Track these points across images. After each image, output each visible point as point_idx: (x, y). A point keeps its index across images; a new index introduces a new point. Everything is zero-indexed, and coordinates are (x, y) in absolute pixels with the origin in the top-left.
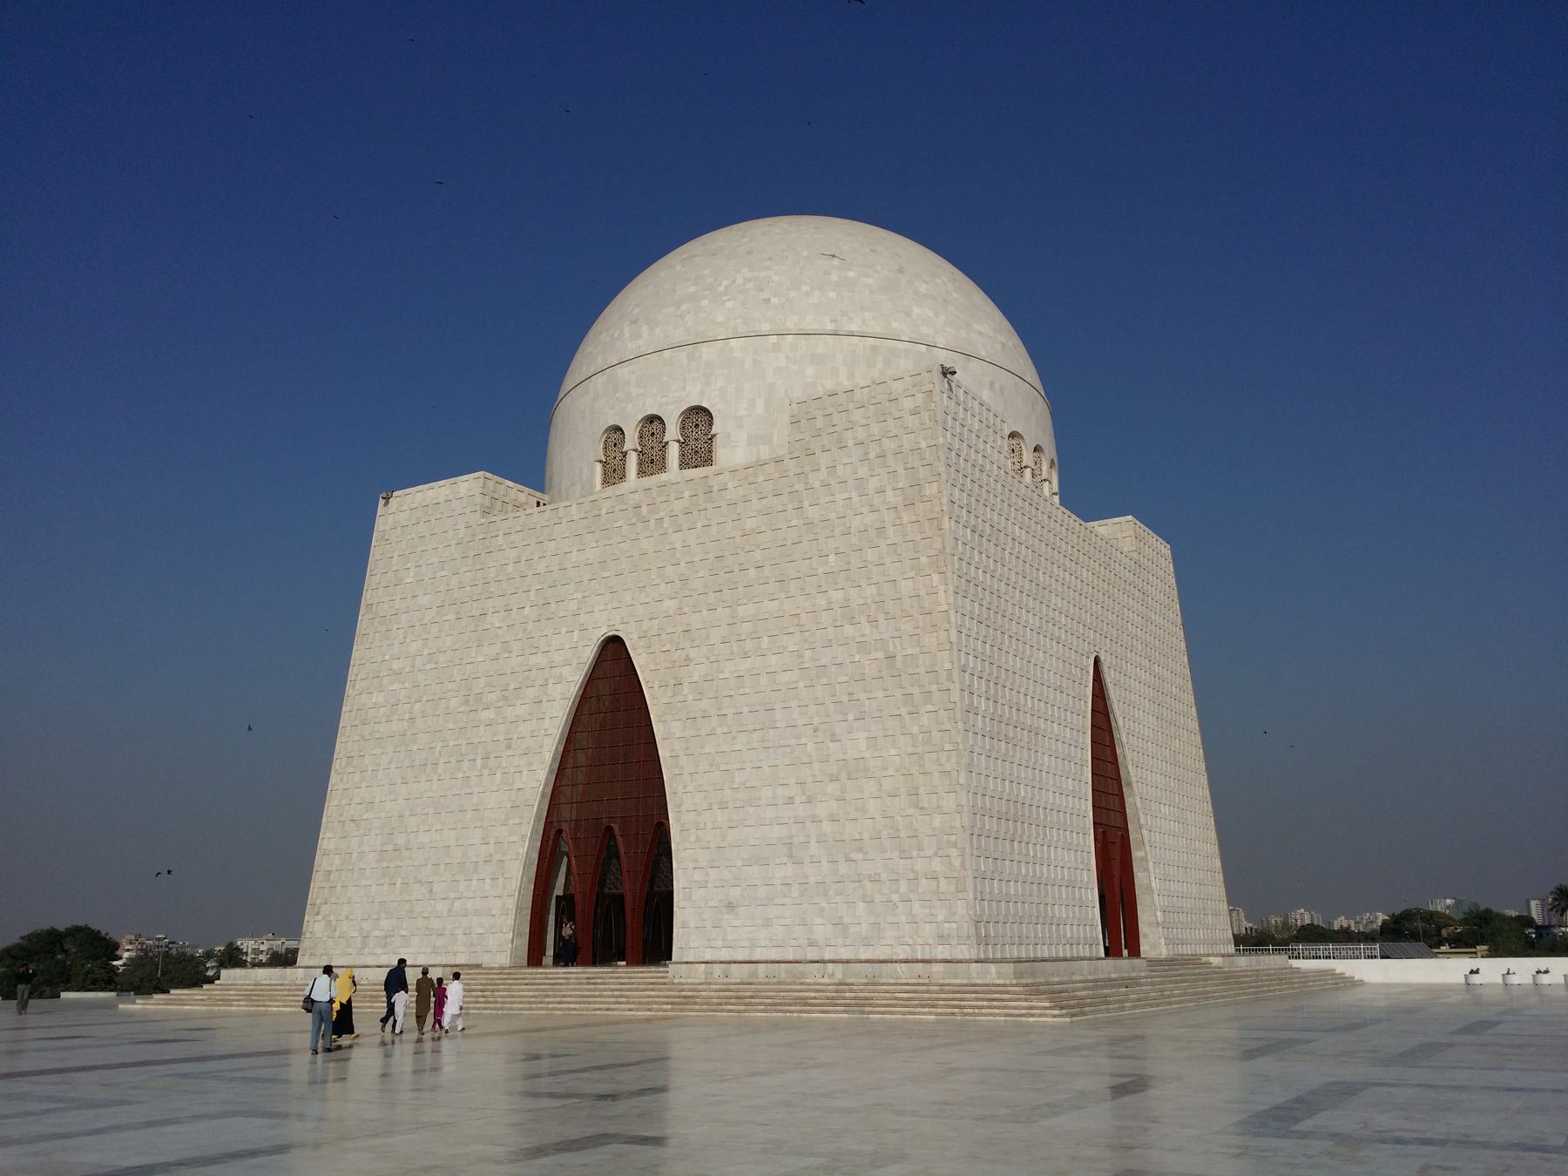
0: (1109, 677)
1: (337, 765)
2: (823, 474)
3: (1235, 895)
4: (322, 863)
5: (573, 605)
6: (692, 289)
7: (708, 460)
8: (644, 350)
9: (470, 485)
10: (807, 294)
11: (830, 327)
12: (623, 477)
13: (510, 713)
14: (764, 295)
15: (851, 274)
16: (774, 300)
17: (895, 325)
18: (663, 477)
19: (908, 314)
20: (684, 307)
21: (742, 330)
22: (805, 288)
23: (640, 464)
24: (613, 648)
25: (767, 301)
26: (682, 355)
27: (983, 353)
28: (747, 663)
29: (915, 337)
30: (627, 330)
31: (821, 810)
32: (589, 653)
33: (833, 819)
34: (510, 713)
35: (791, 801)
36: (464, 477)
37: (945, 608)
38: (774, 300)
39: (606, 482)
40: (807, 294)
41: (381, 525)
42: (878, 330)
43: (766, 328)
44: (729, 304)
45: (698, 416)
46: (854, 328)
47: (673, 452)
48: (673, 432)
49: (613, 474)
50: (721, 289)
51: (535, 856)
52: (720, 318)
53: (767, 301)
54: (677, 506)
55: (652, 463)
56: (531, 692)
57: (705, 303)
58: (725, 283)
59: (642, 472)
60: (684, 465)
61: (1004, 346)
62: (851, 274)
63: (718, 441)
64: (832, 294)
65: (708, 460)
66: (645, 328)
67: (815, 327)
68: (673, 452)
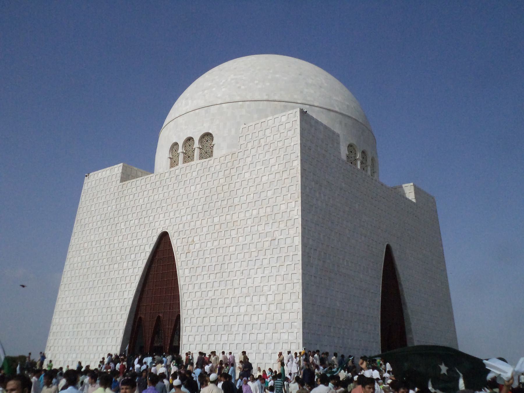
0: (396, 254)
1: (62, 287)
2: (250, 159)
3: (304, 344)
4: (54, 328)
6: (210, 84)
7: (211, 155)
9: (117, 169)
10: (257, 84)
11: (265, 98)
14: (238, 85)
15: (277, 76)
16: (243, 87)
17: (295, 96)
18: (192, 163)
19: (302, 92)
20: (206, 92)
22: (256, 82)
23: (184, 158)
24: (164, 237)
25: (239, 87)
26: (203, 111)
27: (337, 109)
28: (216, 243)
29: (304, 102)
30: (184, 102)
31: (243, 309)
32: (155, 239)
36: (116, 166)
37: (297, 217)
38: (243, 87)
39: (172, 166)
40: (257, 84)
41: (85, 187)
42: (287, 100)
43: (238, 98)
44: (223, 90)
45: (207, 136)
46: (276, 98)
47: (197, 153)
48: (196, 144)
49: (173, 163)
50: (221, 83)
51: (131, 328)
52: (219, 95)
53: (239, 87)
54: (195, 174)
55: (188, 157)
57: (214, 89)
58: (224, 81)
59: (185, 161)
60: (201, 157)
61: (348, 106)
62: (277, 76)
64: (268, 84)
66: (190, 102)
67: (259, 98)
68: (197, 153)
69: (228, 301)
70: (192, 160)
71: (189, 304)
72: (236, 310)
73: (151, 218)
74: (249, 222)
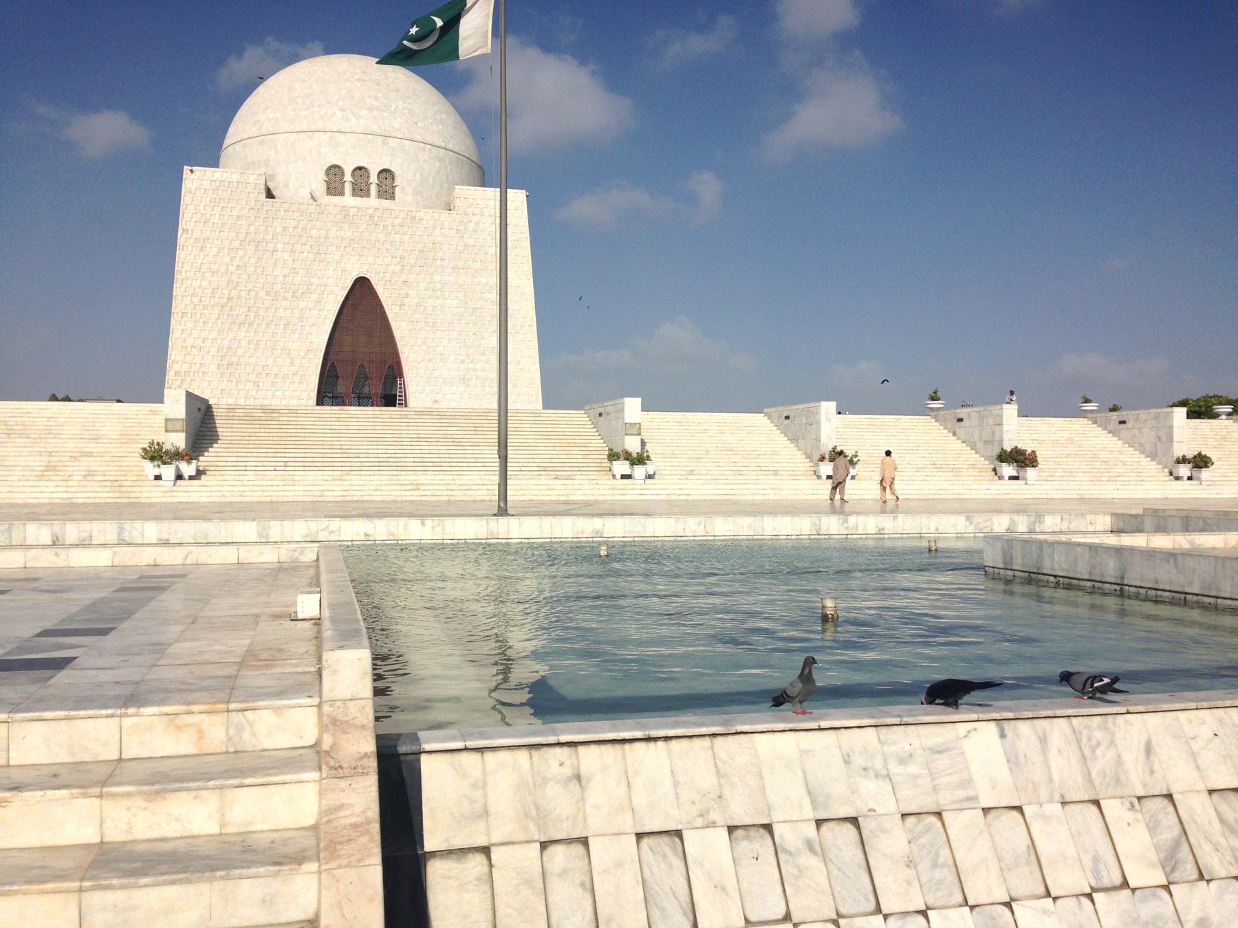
5: (337, 257)
7: (392, 197)
8: (353, 129)
12: (342, 193)
13: (302, 304)
21: (408, 136)
32: (349, 284)
33: (483, 370)
34: (302, 304)
35: (463, 361)
43: (418, 138)
45: (386, 174)
47: (373, 189)
54: (398, 221)
55: (361, 190)
56: (314, 296)
63: (397, 190)
65: (392, 197)
66: (352, 117)
67: (437, 143)
68: (373, 189)
69: (461, 358)
70: (368, 195)
71: (412, 357)
72: (472, 366)
73: (337, 257)
74: (478, 288)
